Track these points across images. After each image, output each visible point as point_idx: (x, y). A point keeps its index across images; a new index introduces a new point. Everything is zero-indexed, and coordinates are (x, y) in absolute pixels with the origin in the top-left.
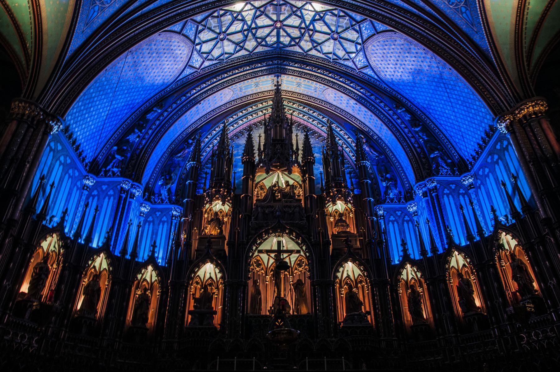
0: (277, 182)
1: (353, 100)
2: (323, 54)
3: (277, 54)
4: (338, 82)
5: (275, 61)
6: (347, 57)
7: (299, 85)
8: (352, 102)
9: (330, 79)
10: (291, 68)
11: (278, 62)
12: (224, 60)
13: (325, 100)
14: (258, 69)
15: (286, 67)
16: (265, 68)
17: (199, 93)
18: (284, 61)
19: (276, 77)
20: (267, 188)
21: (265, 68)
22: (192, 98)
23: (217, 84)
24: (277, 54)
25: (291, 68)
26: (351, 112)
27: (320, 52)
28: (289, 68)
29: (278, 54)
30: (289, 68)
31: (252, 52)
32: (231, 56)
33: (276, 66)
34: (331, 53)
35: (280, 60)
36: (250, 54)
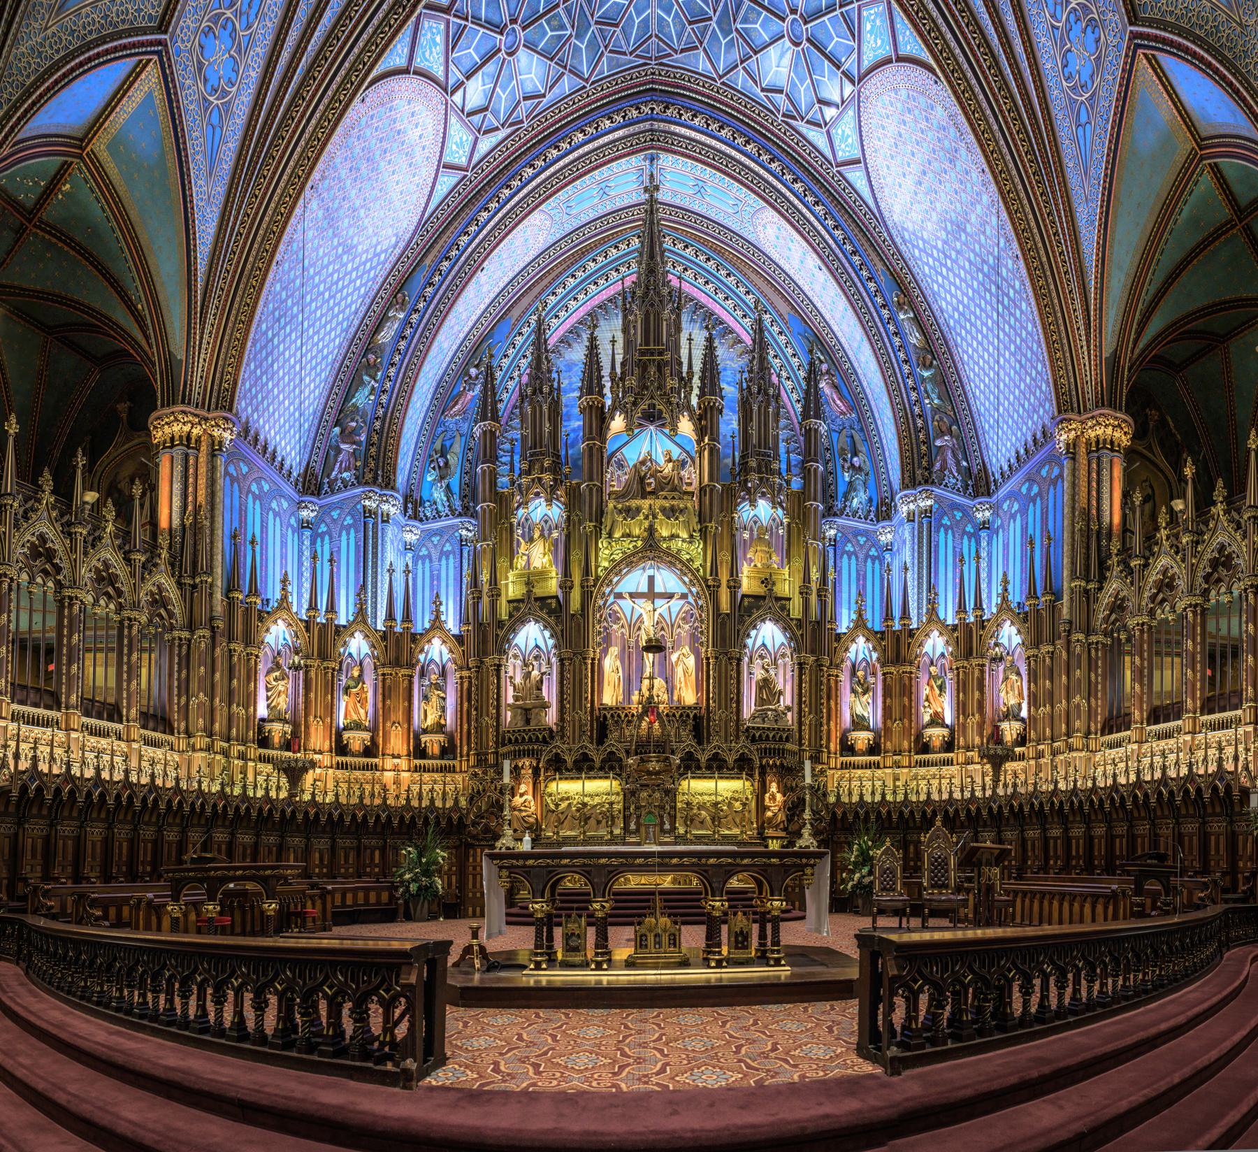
0: (649, 453)
1: (815, 256)
2: (763, 90)
3: (649, 83)
4: (788, 194)
5: (646, 104)
6: (814, 113)
7: (700, 191)
8: (813, 261)
9: (771, 179)
10: (683, 131)
11: (652, 109)
12: (522, 122)
13: (756, 243)
14: (606, 139)
15: (673, 128)
16: (620, 133)
17: (477, 241)
18: (667, 108)
19: (648, 162)
20: (631, 464)
21: (620, 133)
22: (463, 259)
23: (512, 203)
24: (649, 83)
25: (683, 131)
26: (806, 288)
27: (755, 82)
28: (678, 129)
29: (653, 82)
30: (678, 129)
31: (587, 80)
32: (539, 103)
33: (647, 125)
34: (781, 92)
35: (658, 102)
36: (584, 87)
